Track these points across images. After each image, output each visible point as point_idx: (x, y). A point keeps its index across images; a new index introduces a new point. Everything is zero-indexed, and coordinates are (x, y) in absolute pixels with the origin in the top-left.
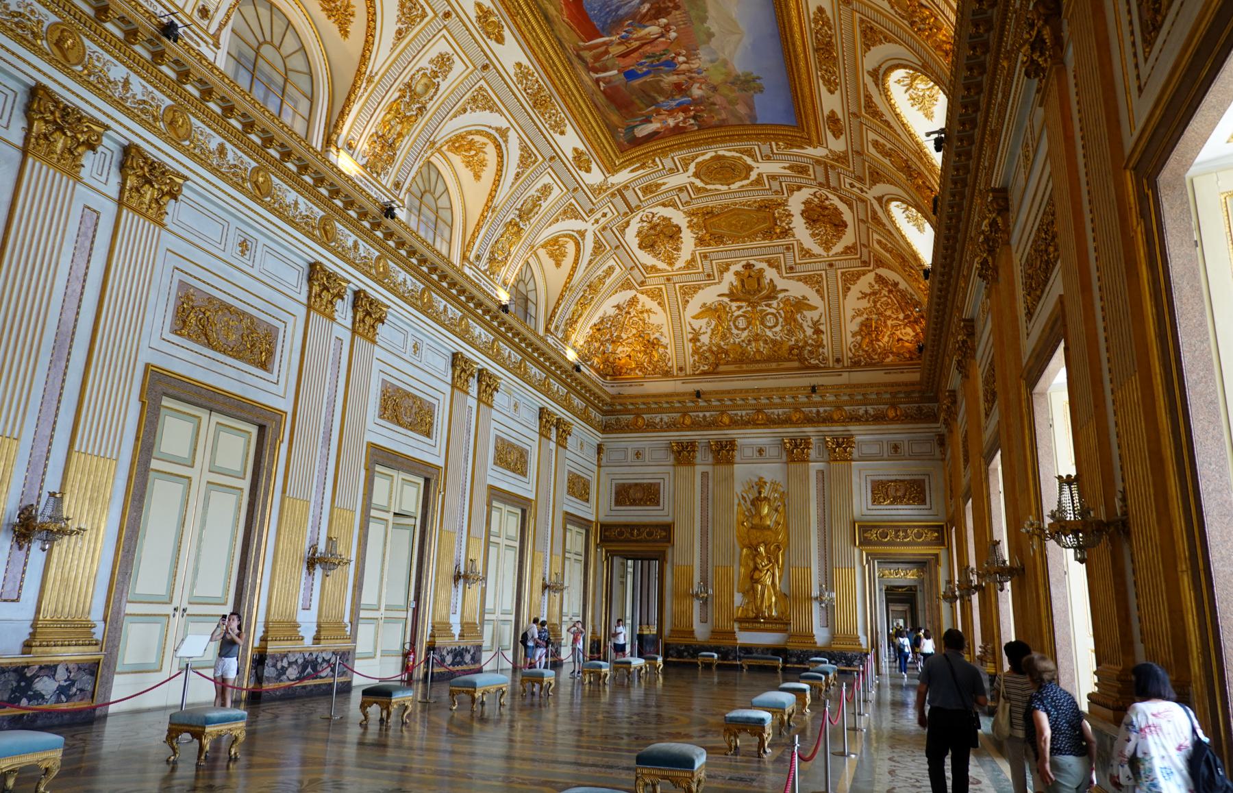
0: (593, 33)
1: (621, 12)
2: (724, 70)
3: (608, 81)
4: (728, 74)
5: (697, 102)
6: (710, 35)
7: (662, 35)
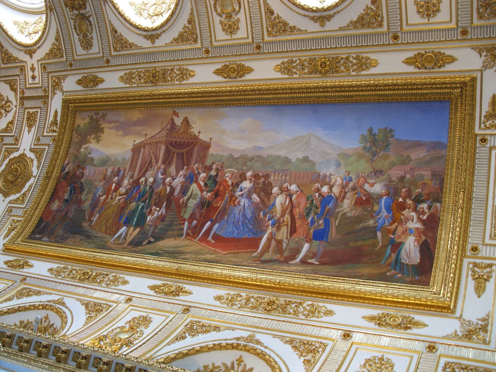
0: (254, 243)
1: (249, 215)
2: (353, 159)
3: (312, 254)
4: (360, 156)
5: (393, 191)
6: (306, 160)
7: (290, 196)
